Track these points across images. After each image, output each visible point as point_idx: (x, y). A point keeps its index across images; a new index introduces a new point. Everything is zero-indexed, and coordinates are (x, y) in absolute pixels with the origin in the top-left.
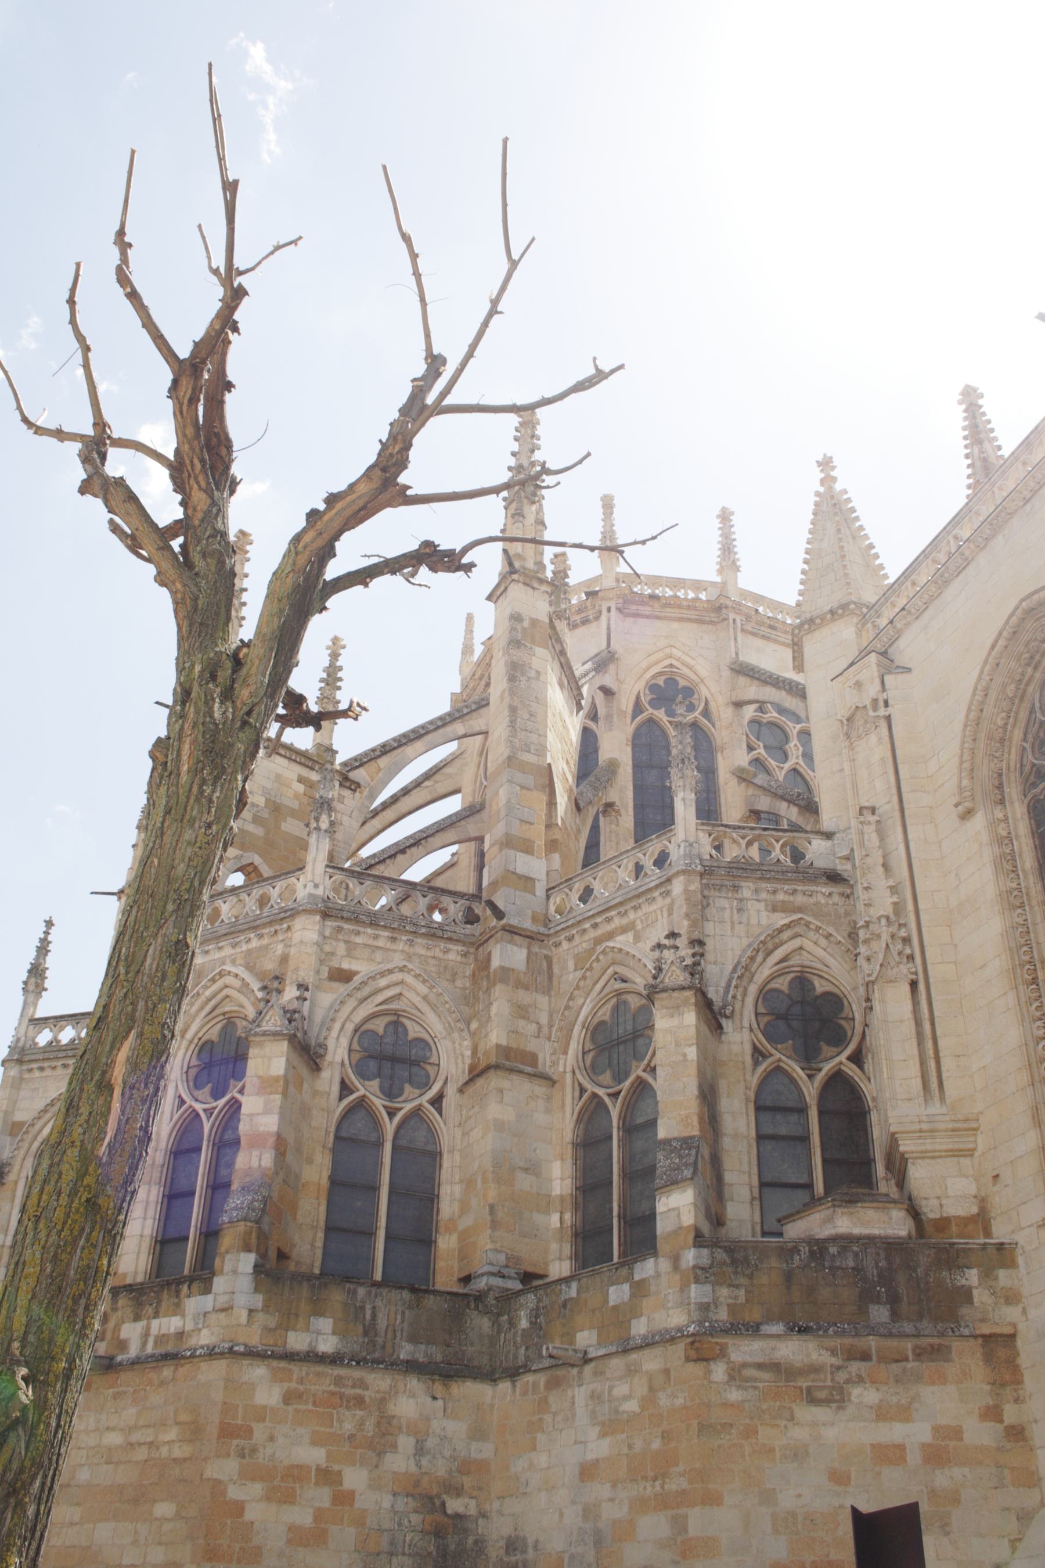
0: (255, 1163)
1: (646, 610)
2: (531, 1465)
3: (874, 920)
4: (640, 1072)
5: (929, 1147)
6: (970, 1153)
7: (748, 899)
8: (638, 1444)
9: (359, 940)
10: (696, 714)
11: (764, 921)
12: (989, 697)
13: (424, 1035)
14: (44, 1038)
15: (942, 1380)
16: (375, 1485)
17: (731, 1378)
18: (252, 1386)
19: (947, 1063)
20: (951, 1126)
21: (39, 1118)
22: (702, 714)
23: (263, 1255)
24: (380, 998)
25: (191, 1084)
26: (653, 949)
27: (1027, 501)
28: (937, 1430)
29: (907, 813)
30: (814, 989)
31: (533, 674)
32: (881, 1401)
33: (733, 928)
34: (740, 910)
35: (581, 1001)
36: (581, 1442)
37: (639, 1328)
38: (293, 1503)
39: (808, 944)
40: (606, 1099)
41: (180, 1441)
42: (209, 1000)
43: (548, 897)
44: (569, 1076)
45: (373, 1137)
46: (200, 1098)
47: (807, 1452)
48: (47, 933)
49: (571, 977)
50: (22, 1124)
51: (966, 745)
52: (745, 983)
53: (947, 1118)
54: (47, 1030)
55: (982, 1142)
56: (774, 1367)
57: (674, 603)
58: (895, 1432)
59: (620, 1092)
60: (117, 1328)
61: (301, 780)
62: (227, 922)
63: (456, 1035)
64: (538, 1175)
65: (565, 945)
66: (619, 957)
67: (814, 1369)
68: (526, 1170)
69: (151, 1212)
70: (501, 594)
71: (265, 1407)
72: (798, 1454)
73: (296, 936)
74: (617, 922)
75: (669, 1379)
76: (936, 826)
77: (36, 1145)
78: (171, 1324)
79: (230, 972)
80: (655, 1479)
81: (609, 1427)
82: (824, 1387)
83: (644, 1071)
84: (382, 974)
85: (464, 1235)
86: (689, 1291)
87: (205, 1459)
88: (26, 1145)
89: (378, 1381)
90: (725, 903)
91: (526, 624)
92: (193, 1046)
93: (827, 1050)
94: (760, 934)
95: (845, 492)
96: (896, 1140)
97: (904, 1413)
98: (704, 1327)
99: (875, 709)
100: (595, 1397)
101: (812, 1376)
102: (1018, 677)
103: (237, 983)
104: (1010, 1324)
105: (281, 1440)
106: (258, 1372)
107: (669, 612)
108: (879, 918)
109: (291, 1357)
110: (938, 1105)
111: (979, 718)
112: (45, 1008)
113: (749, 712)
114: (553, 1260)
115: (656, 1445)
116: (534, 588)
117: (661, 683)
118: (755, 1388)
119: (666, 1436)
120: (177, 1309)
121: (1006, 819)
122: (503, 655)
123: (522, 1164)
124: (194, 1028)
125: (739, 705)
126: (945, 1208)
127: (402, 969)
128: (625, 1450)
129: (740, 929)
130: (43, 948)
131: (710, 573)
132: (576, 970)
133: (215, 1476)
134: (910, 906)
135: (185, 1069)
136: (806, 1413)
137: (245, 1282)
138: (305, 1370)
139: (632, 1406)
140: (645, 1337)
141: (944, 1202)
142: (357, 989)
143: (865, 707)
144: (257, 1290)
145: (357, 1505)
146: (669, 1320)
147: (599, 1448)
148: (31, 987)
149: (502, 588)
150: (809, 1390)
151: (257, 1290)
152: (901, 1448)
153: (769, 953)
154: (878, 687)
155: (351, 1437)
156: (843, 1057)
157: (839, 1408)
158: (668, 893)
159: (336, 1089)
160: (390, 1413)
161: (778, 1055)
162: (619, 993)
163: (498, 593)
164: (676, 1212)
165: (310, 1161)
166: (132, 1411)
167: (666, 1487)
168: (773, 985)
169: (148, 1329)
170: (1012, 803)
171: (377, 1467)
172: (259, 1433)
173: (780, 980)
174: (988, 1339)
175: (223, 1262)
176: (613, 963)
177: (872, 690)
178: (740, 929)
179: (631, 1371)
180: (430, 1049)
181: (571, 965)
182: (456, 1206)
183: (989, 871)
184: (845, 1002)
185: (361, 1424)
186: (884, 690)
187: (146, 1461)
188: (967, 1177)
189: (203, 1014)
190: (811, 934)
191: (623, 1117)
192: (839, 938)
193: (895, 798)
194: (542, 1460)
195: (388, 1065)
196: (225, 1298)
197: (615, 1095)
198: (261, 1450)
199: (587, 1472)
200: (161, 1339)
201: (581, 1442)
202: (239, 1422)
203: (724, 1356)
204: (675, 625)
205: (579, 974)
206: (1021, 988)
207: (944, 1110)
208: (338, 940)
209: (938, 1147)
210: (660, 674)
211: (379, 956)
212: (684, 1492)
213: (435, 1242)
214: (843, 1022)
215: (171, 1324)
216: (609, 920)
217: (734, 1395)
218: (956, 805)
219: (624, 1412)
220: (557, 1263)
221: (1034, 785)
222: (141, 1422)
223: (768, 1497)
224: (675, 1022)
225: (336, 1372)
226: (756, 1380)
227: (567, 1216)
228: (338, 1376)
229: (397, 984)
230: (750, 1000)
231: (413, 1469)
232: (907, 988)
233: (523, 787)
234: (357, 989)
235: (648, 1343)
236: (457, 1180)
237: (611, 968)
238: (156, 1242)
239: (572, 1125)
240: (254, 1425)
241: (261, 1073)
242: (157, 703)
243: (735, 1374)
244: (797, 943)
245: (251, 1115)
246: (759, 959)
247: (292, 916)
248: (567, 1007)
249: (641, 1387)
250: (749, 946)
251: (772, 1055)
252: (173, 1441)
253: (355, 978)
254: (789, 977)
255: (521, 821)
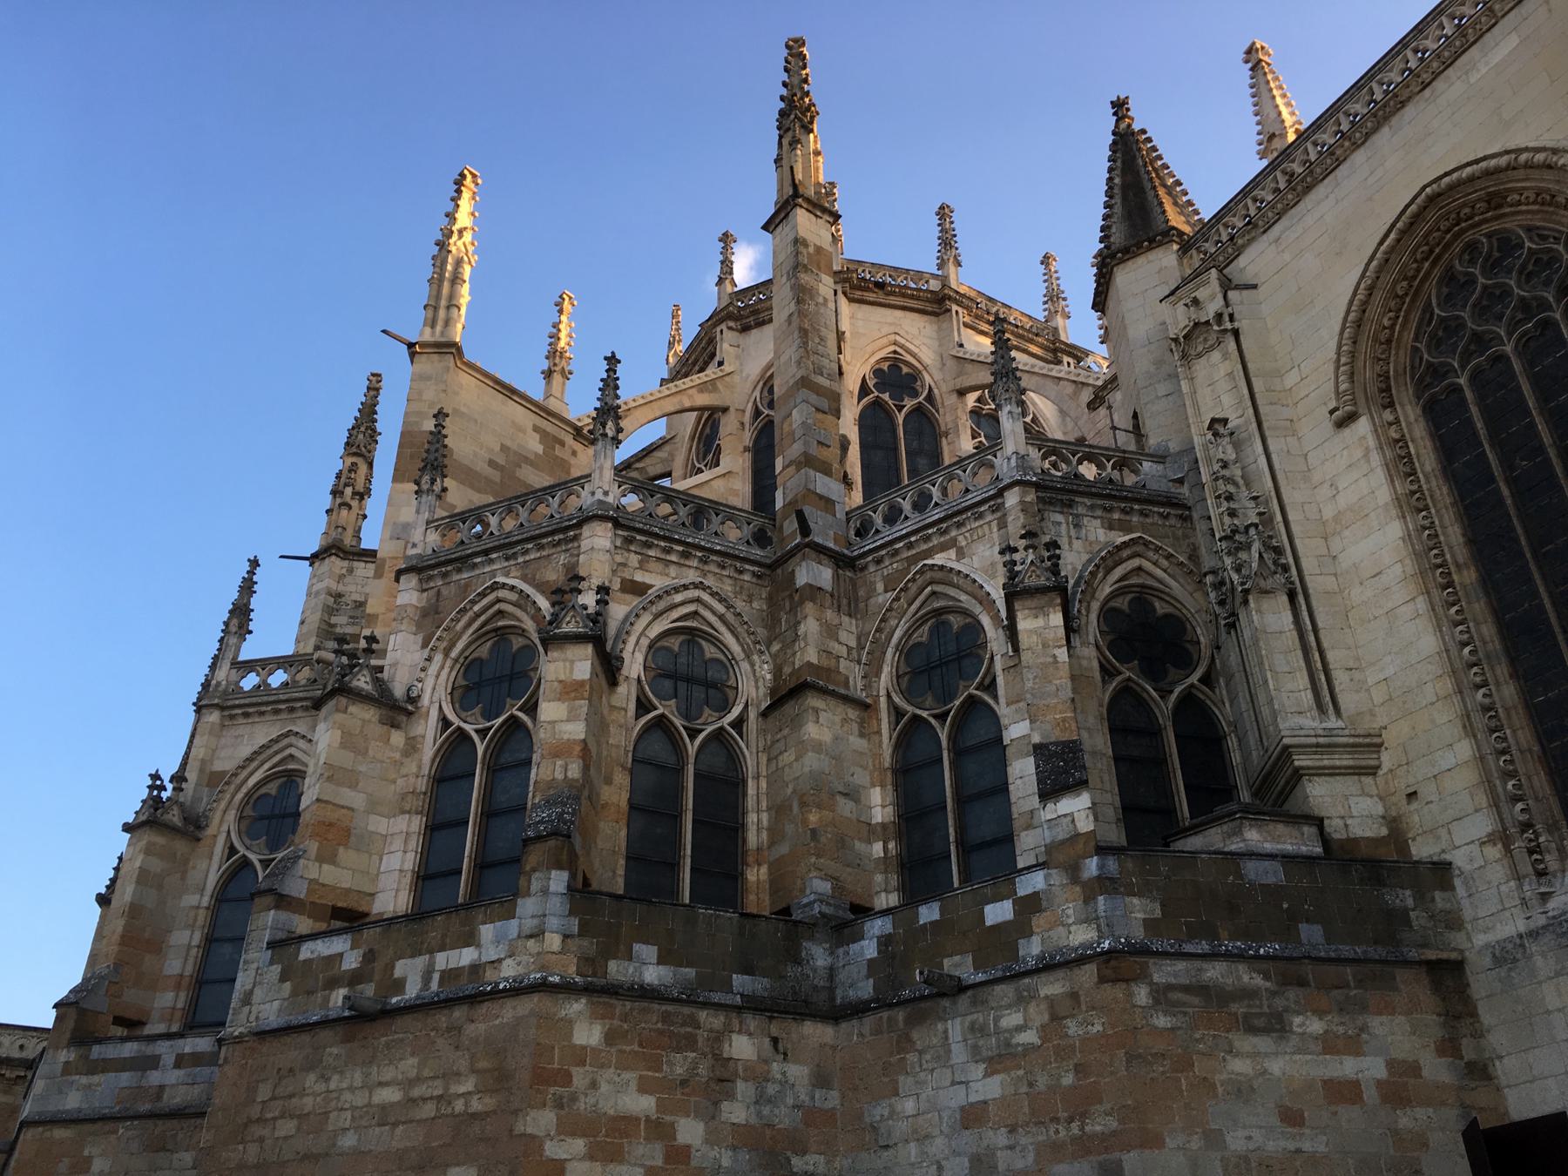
0: (559, 776)
1: (871, 296)
2: (893, 1113)
3: (1242, 529)
4: (972, 691)
5: (1326, 763)
6: (1372, 771)
7: (1083, 515)
8: (1042, 1082)
9: (651, 553)
10: (921, 399)
11: (1102, 538)
12: (1373, 298)
13: (722, 657)
14: (250, 682)
15: (1390, 1010)
16: (711, 1139)
17: (1157, 1002)
18: (569, 1023)
19: (1340, 677)
20: (1351, 740)
21: (243, 767)
22: (925, 399)
23: (573, 876)
24: (675, 614)
25: (457, 706)
26: (1002, 552)
27: (1425, 86)
28: (1391, 1064)
29: (1265, 425)
30: (1154, 610)
31: (821, 300)
32: (1326, 1032)
33: (1070, 543)
34: (1077, 526)
35: (893, 622)
36: (962, 1083)
37: (1032, 948)
38: (621, 1162)
39: (1147, 565)
40: (933, 721)
41: (479, 1092)
42: (478, 615)
43: (848, 521)
44: (883, 700)
45: (671, 760)
46: (469, 719)
47: (1253, 1090)
48: (251, 573)
49: (881, 599)
50: (224, 773)
51: (1345, 348)
52: (1088, 598)
53: (1347, 732)
54: (253, 675)
55: (1387, 760)
56: (1202, 990)
57: (903, 292)
58: (1348, 1067)
59: (947, 713)
60: (391, 967)
61: (536, 429)
62: (497, 533)
63: (755, 657)
64: (857, 801)
65: (872, 568)
66: (939, 575)
67: (1249, 994)
68: (846, 795)
69: (413, 844)
70: (781, 221)
71: (584, 1048)
72: (1242, 1091)
73: (585, 544)
74: (935, 541)
75: (1079, 1003)
76: (1299, 439)
77: (240, 796)
78: (467, 956)
79: (504, 584)
80: (1071, 1120)
81: (995, 1063)
82: (1261, 1015)
83: (977, 689)
84: (677, 590)
85: (777, 867)
86: (1096, 903)
87: (516, 1112)
88: (228, 796)
89: (710, 1020)
90: (1059, 518)
91: (811, 249)
92: (458, 666)
93: (1173, 673)
94: (1100, 550)
95: (1143, 131)
96: (1290, 755)
97: (1353, 1046)
98: (1120, 943)
99: (1219, 323)
100: (977, 1030)
101: (1246, 1002)
102: (1410, 274)
103: (513, 597)
104: (1454, 949)
105: (604, 1088)
106: (576, 1007)
107: (892, 300)
108: (1247, 528)
109: (613, 991)
110: (1333, 718)
111: (1361, 319)
112: (249, 651)
113: (971, 399)
114: (877, 893)
115: (1068, 1080)
116: (816, 216)
117: (886, 368)
118: (1185, 1014)
119: (1079, 1069)
120: (470, 939)
121: (1397, 421)
122: (789, 279)
123: (841, 789)
124: (460, 645)
125: (962, 393)
126: (1351, 828)
127: (696, 586)
128: (1024, 1089)
129: (1077, 544)
130: (248, 587)
131: (930, 266)
132: (886, 591)
133: (529, 1130)
134: (1279, 518)
135: (449, 691)
136: (1245, 1043)
137: (557, 905)
138: (628, 1005)
139: (1030, 1037)
140: (1041, 957)
141: (1349, 822)
142: (652, 602)
143: (1207, 322)
144: (572, 913)
145: (694, 1163)
146: (1071, 937)
147: (989, 1088)
148: (233, 629)
149: (783, 215)
150: (1246, 1016)
151: (572, 913)
152: (1356, 1084)
153: (1109, 571)
154: (1222, 302)
155: (684, 1083)
156: (1194, 678)
157: (1281, 1038)
158: (998, 508)
159: (632, 706)
160: (725, 1055)
161: (1128, 674)
162: (938, 612)
163: (777, 221)
164: (1069, 818)
165: (608, 781)
166: (413, 1061)
167: (1088, 1128)
168: (1112, 604)
169: (431, 964)
170: (1403, 406)
171: (713, 1118)
172: (580, 1077)
173: (1120, 600)
174: (1434, 966)
175: (529, 881)
176: (930, 583)
177: (1213, 307)
178: (1077, 544)
179: (1021, 1001)
180: (728, 673)
181: (880, 587)
182: (764, 835)
183: (1380, 476)
184: (1188, 626)
185: (694, 1066)
186: (1227, 304)
187: (433, 1119)
188: (1371, 796)
189: (471, 631)
190: (1151, 554)
191: (952, 738)
192: (1181, 559)
193: (1251, 411)
194: (909, 1106)
195: (682, 686)
196: (536, 921)
197: (942, 717)
198: (582, 1098)
199: (972, 1116)
200: (449, 975)
201: (962, 1083)
202: (556, 1066)
203: (1146, 977)
204: (899, 313)
205: (891, 595)
206: (1435, 592)
207: (1340, 724)
208: (629, 551)
209: (1338, 763)
210: (885, 359)
211: (673, 571)
212: (1114, 1133)
213: (742, 874)
214: (1188, 646)
215: (467, 956)
216: (927, 539)
217: (1162, 1021)
218: (1332, 412)
219: (1018, 1044)
220: (883, 894)
221: (1428, 386)
222: (426, 1073)
223: (1214, 1139)
224: (1040, 622)
225: (664, 1008)
226: (1184, 1004)
227: (891, 845)
228: (666, 1011)
229: (691, 601)
230: (1093, 617)
231: (753, 1120)
232: (1285, 598)
233: (818, 410)
234: (652, 602)
235: (1047, 966)
236: (764, 808)
237: (929, 588)
238: (418, 877)
239: (890, 751)
240: (575, 1071)
241: (562, 677)
242: (384, 331)
243: (1161, 995)
244: (1136, 562)
245: (553, 723)
246: (1100, 575)
247: (580, 525)
248: (879, 630)
249: (1039, 1015)
250: (1090, 561)
251: (1120, 673)
252: (470, 1093)
253: (650, 592)
254: (1129, 597)
255: (819, 442)
